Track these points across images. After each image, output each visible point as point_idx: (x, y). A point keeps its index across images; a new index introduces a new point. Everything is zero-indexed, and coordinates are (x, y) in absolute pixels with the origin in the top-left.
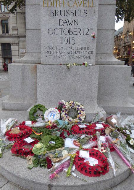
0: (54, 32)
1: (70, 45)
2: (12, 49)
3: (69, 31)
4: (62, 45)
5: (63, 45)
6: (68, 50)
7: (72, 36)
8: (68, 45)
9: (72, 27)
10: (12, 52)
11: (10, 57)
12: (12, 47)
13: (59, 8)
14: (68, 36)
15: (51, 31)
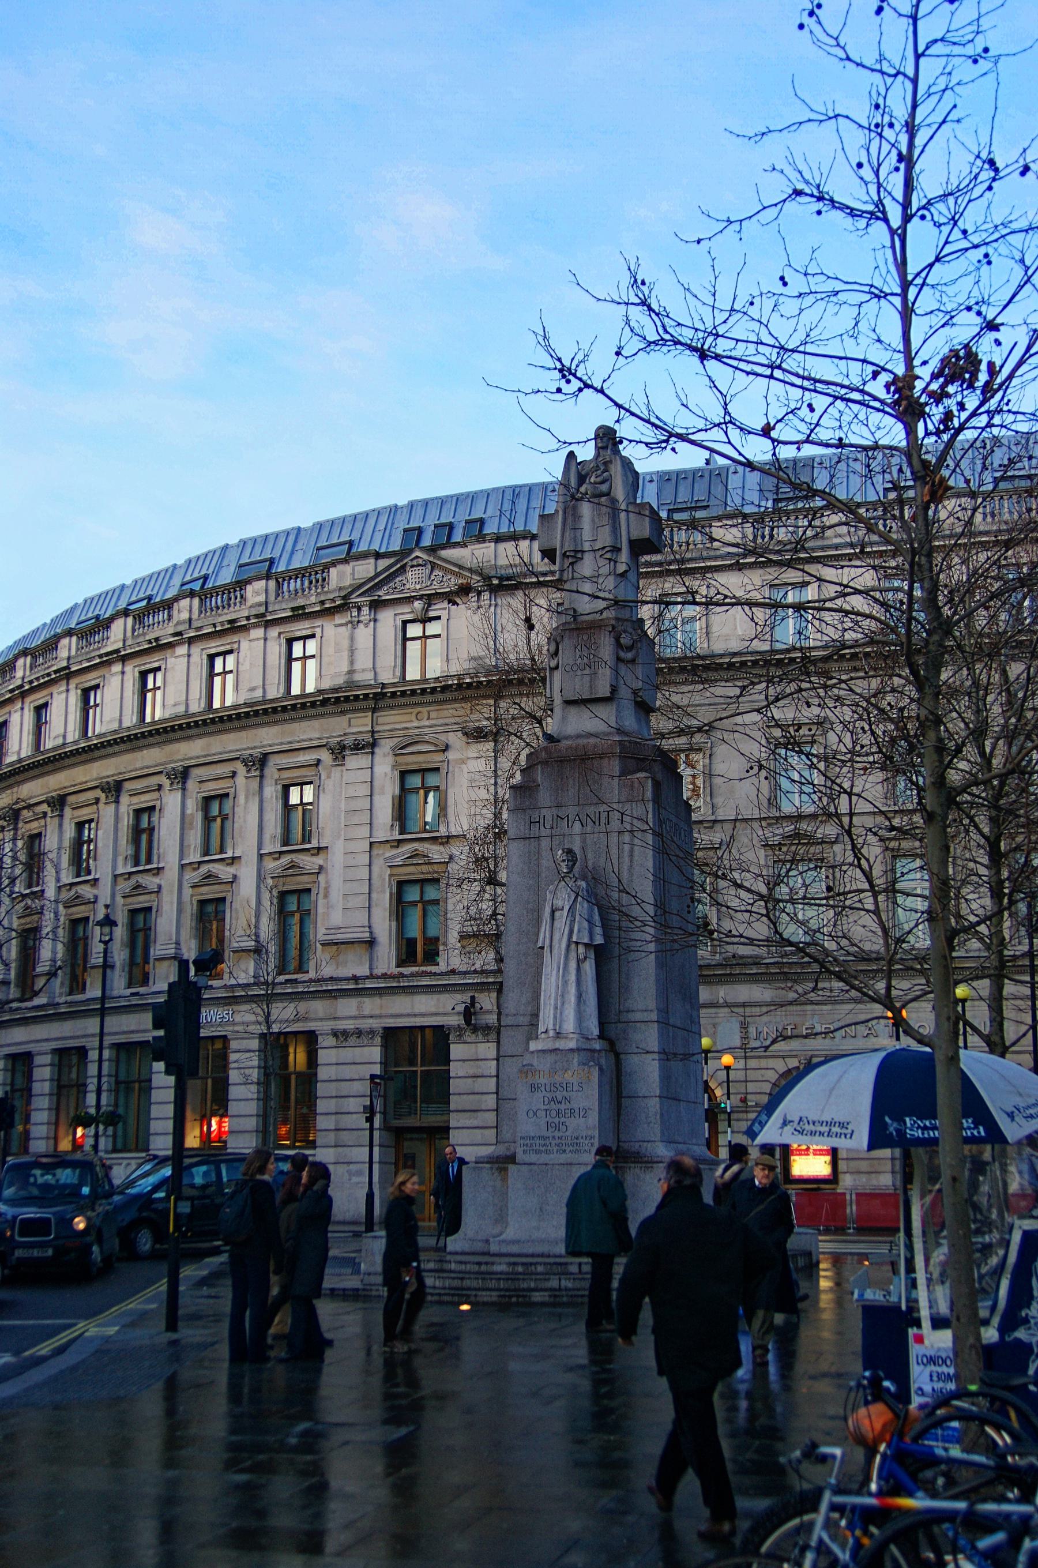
0: (535, 1114)
1: (560, 1134)
2: (455, 1069)
3: (558, 1114)
4: (546, 1134)
5: (549, 1134)
6: (557, 1141)
7: (563, 1120)
8: (557, 1134)
9: (562, 1107)
10: (454, 1085)
11: (432, 1120)
12: (456, 1050)
13: (543, 1081)
14: (556, 1120)
15: (531, 1114)
